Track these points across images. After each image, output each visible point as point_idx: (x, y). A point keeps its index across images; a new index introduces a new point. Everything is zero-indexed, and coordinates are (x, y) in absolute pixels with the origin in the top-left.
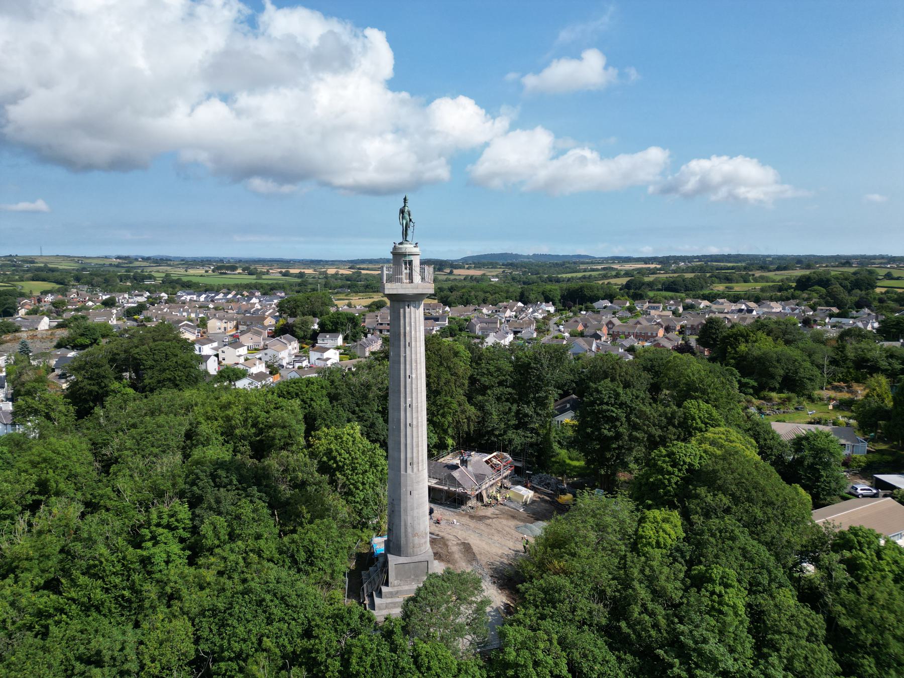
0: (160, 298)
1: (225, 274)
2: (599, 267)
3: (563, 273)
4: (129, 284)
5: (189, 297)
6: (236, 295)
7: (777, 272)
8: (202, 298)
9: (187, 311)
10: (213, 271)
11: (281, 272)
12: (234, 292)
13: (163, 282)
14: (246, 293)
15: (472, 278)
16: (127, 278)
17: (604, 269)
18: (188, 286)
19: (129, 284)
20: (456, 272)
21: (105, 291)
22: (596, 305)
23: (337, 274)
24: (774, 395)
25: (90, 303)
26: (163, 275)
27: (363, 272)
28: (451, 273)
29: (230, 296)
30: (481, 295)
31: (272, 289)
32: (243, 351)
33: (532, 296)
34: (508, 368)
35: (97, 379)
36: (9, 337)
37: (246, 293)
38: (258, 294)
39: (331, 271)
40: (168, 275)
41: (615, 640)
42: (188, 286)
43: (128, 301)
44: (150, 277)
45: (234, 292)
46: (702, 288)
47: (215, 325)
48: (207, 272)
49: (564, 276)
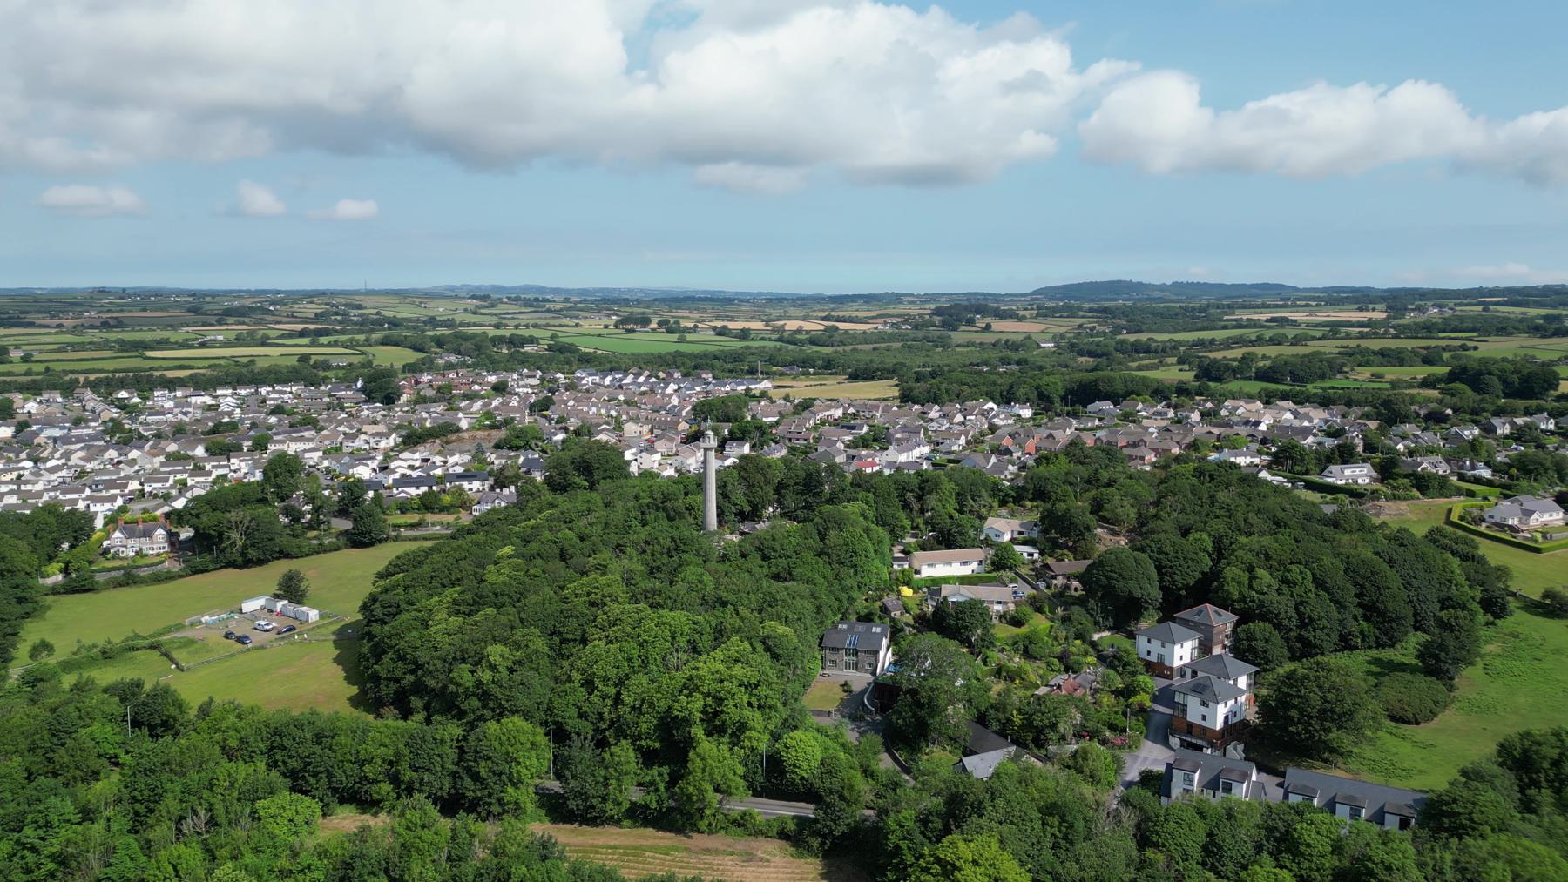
0: (556, 380)
1: (633, 331)
2: (1264, 317)
3: (1185, 330)
4: (505, 351)
5: (590, 379)
6: (650, 377)
7: (1555, 340)
8: (608, 381)
9: (594, 405)
10: (616, 326)
11: (714, 328)
12: (647, 373)
13: (550, 348)
14: (662, 375)
15: (1014, 347)
16: (499, 340)
17: (1272, 320)
18: (587, 361)
19: (505, 351)
20: (997, 325)
21: (491, 371)
22: (1090, 407)
23: (799, 331)
24: (1029, 504)
25: (476, 387)
26: (548, 334)
27: (841, 326)
28: (988, 327)
29: (641, 380)
30: (955, 388)
31: (696, 367)
32: (657, 457)
33: (1021, 392)
34: (802, 474)
35: (563, 474)
36: (454, 437)
37: (662, 375)
38: (677, 375)
39: (792, 325)
40: (553, 337)
41: (758, 549)
42: (587, 361)
43: (525, 385)
44: (532, 340)
45: (647, 373)
46: (1323, 377)
47: (631, 429)
48: (606, 327)
49: (1162, 337)
